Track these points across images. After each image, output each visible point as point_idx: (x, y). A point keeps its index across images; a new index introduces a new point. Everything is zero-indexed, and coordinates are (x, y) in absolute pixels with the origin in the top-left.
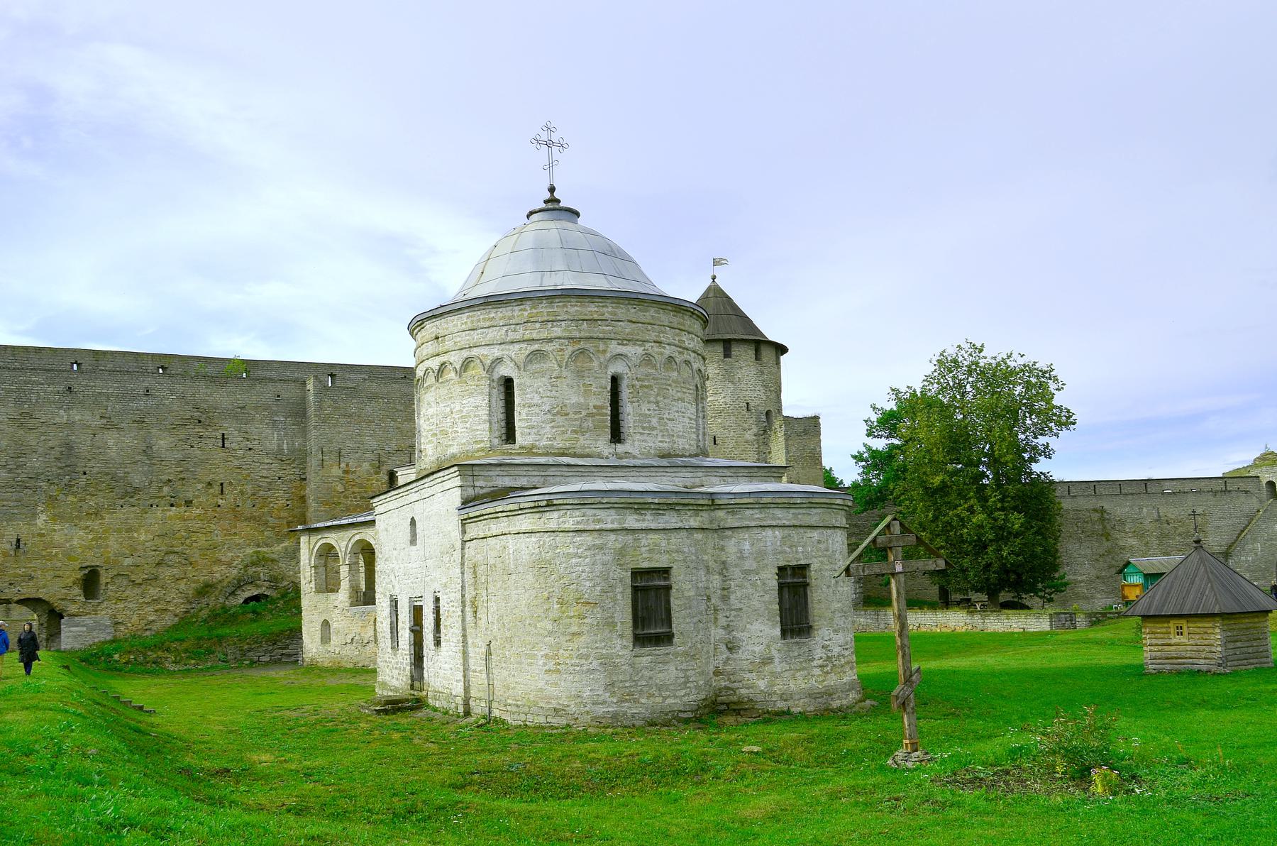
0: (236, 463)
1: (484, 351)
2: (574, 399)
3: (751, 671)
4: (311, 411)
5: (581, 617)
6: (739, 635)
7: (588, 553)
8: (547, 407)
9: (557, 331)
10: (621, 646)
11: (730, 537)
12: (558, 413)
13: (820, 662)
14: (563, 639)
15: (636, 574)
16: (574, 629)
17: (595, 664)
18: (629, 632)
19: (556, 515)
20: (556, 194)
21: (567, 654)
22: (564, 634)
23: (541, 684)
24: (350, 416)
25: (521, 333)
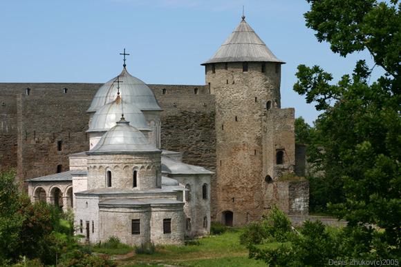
2: (125, 177)
4: (20, 112)
9: (121, 161)
10: (129, 234)
15: (133, 220)
24: (40, 114)
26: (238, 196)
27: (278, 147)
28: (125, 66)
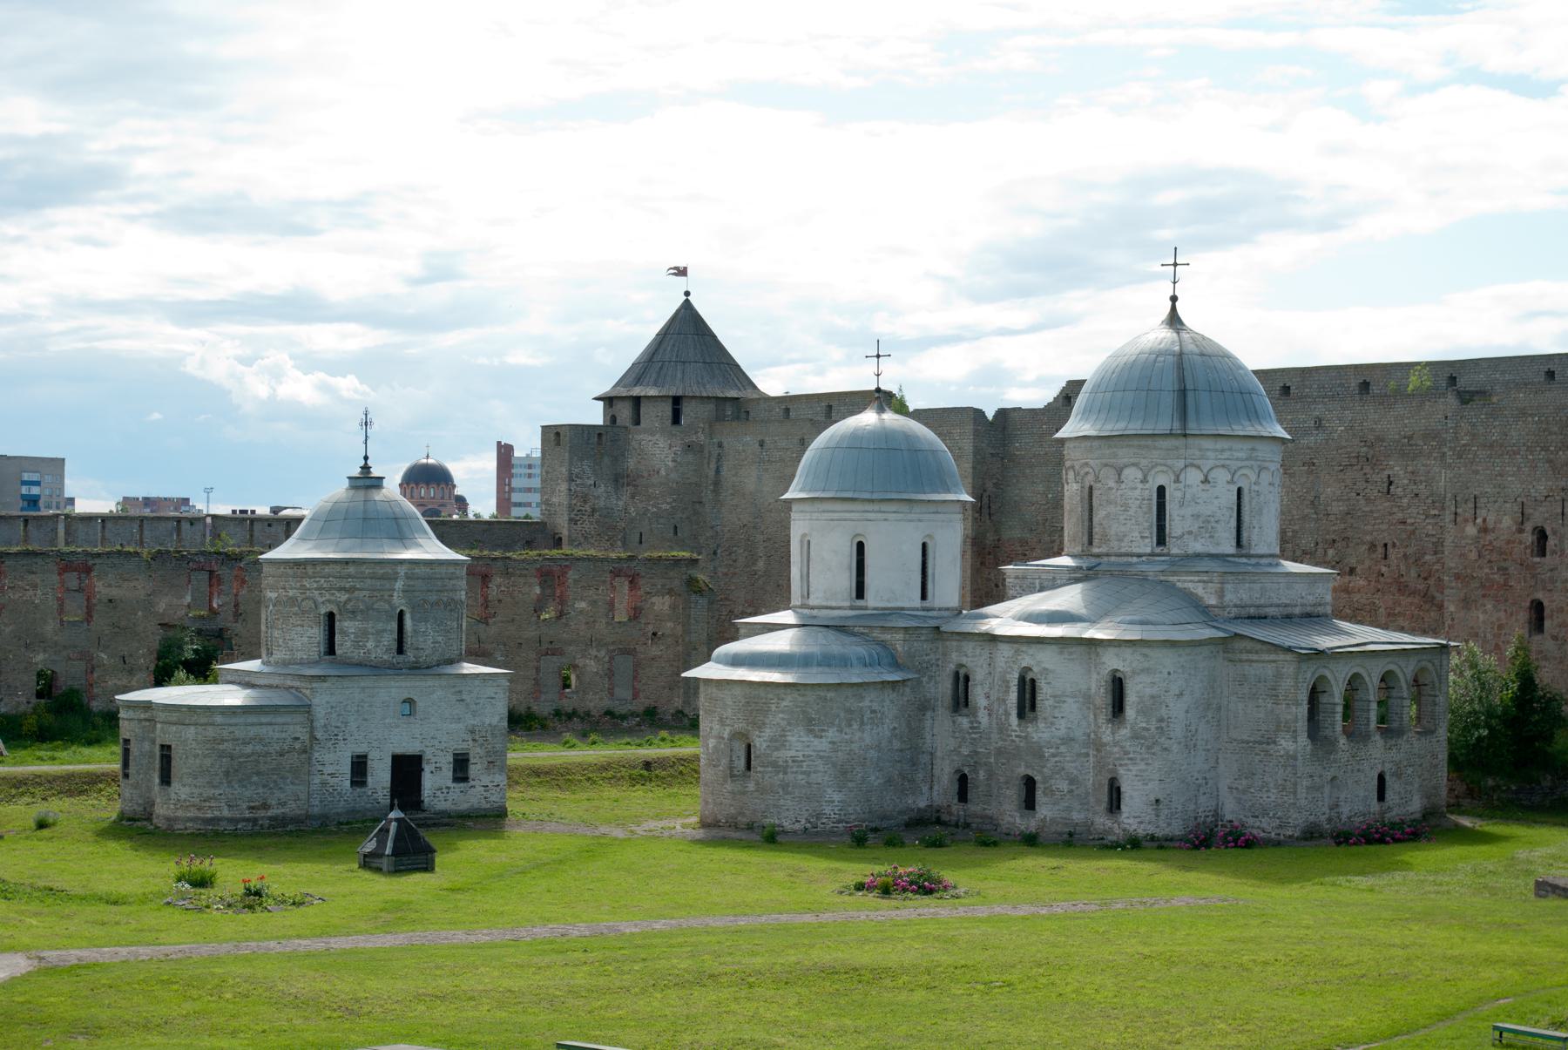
0: (1400, 516)
28: (1174, 299)
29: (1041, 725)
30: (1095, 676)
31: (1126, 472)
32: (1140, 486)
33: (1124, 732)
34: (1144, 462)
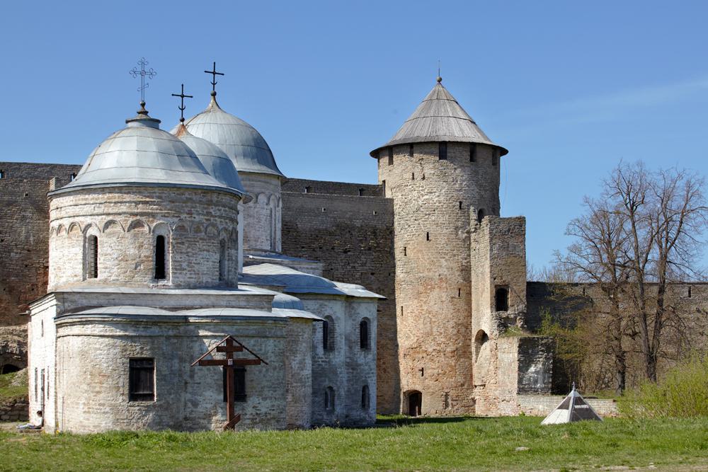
1: (81, 219)
3: (204, 419)
5: (101, 383)
6: (198, 398)
7: (106, 348)
8: (115, 256)
9: (124, 208)
10: (122, 400)
11: (196, 341)
12: (122, 260)
13: (251, 417)
14: (92, 395)
15: (132, 361)
16: (97, 389)
17: (108, 409)
18: (127, 392)
19: (90, 326)
20: (146, 108)
21: (94, 403)
22: (92, 392)
23: (82, 419)
25: (102, 209)
26: (431, 365)
27: (498, 281)
29: (337, 353)
30: (350, 322)
31: (259, 197)
32: (266, 207)
33: (370, 356)
34: (267, 192)
